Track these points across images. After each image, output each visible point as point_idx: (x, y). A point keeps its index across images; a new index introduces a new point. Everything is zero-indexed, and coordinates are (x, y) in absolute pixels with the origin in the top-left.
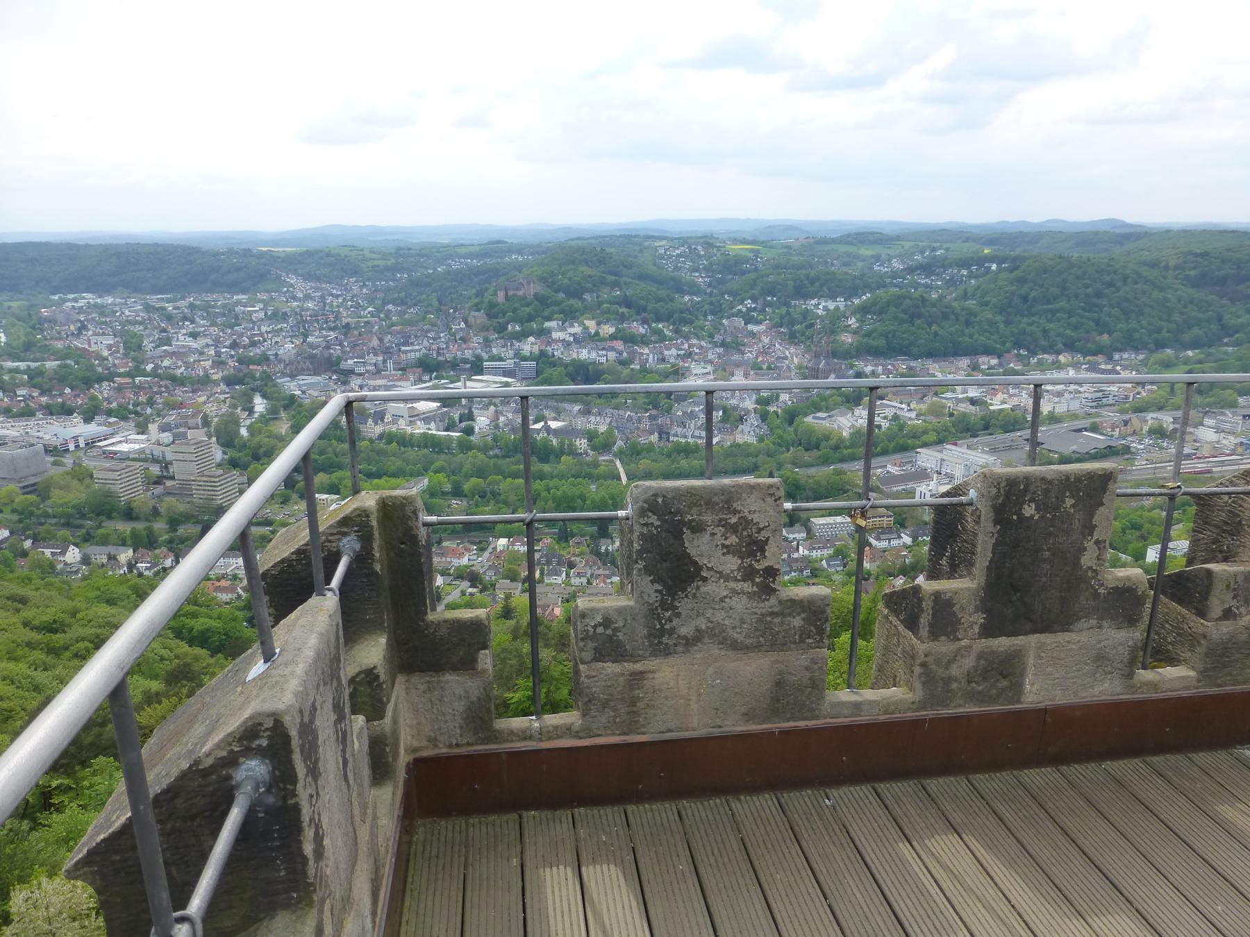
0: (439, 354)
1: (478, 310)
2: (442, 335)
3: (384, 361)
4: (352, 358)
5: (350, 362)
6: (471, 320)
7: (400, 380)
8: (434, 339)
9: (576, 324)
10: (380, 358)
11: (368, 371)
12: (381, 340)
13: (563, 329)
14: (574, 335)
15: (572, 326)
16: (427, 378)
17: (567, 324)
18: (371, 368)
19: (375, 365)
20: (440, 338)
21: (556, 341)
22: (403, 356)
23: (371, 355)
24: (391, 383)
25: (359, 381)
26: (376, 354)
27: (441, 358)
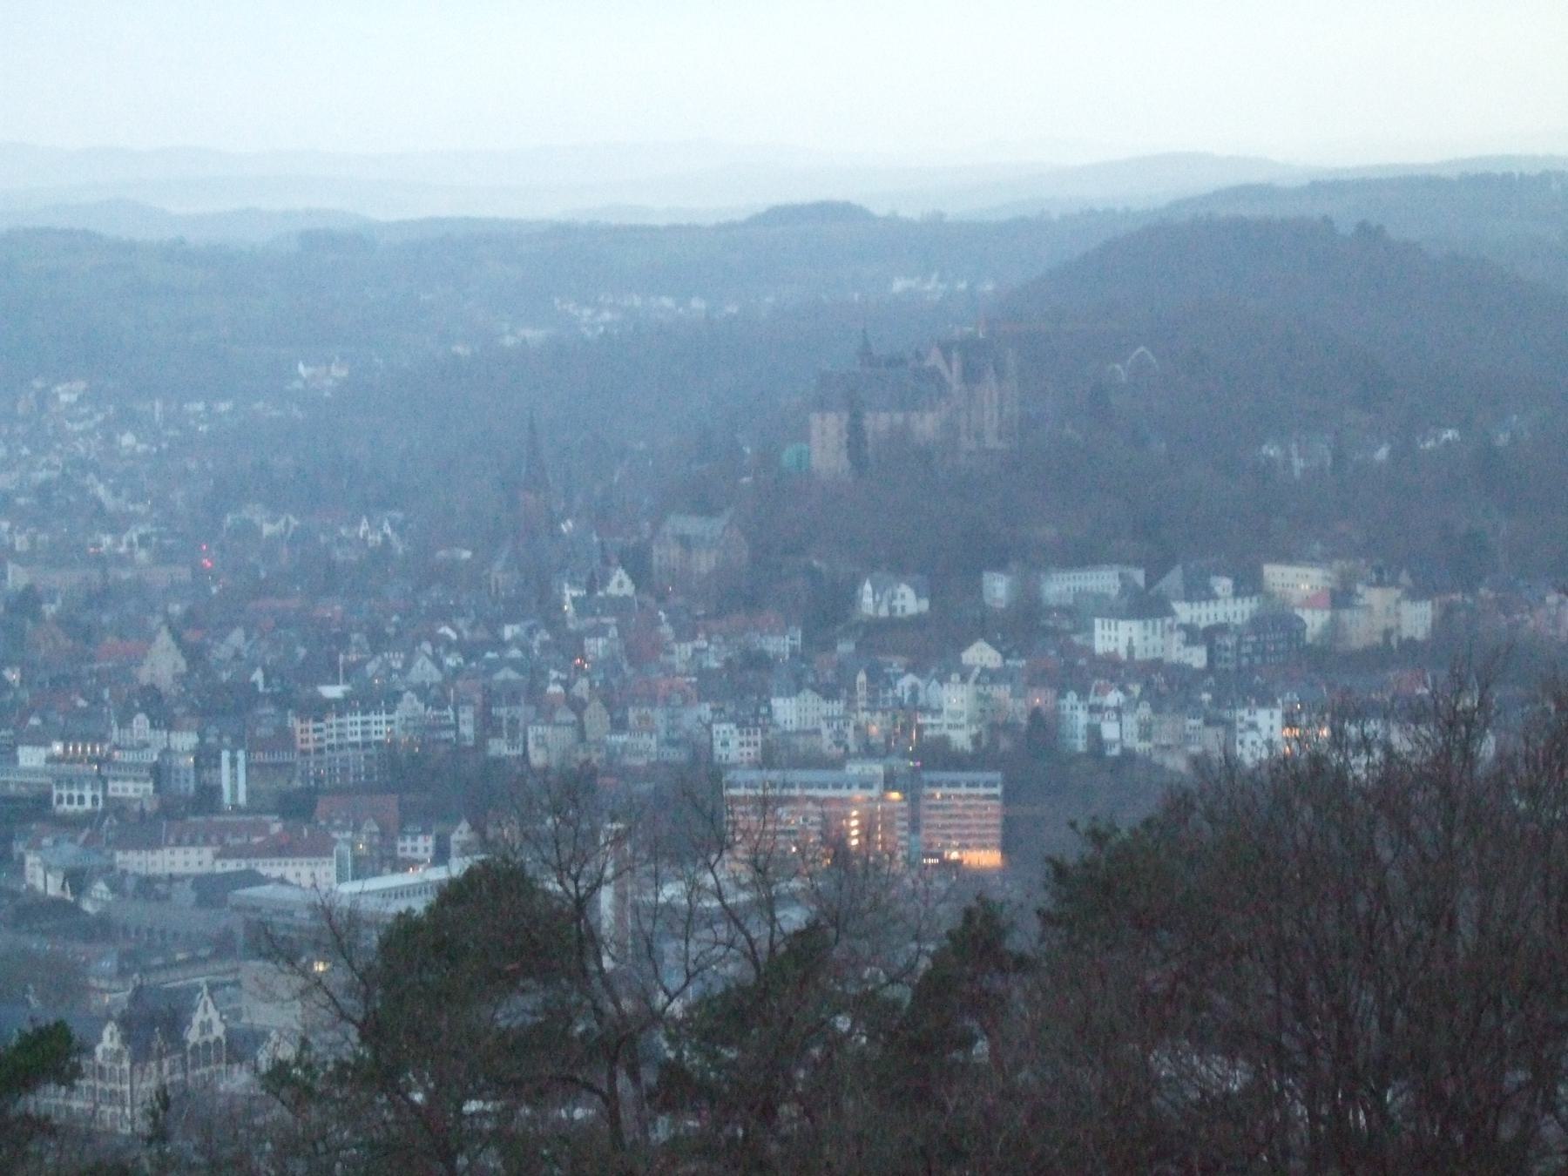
0: (488, 725)
1: (706, 508)
2: (509, 631)
3: (206, 757)
4: (39, 739)
5: (30, 757)
6: (664, 555)
7: (281, 850)
8: (470, 651)
9: (1223, 585)
10: (185, 740)
11: (118, 808)
12: (194, 655)
13: (1145, 606)
14: (1207, 636)
15: (1198, 591)
16: (424, 845)
17: (1174, 579)
18: (134, 790)
19: (158, 773)
20: (501, 645)
21: (1113, 669)
22: (304, 732)
23: (141, 721)
24: (231, 866)
25: (70, 851)
26: (163, 719)
27: (499, 747)
